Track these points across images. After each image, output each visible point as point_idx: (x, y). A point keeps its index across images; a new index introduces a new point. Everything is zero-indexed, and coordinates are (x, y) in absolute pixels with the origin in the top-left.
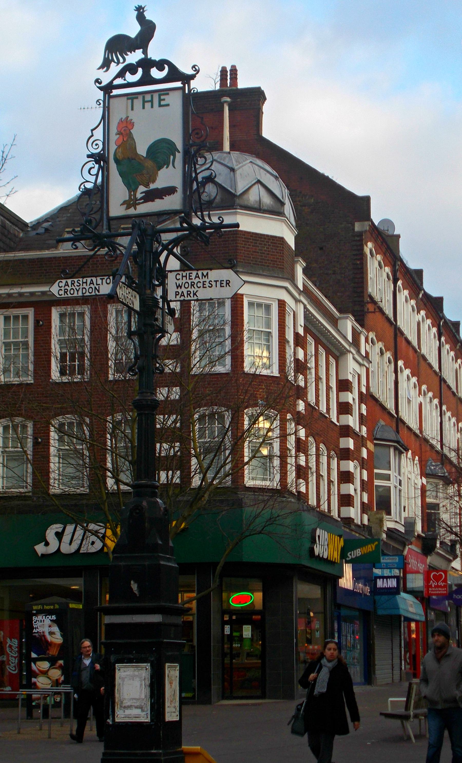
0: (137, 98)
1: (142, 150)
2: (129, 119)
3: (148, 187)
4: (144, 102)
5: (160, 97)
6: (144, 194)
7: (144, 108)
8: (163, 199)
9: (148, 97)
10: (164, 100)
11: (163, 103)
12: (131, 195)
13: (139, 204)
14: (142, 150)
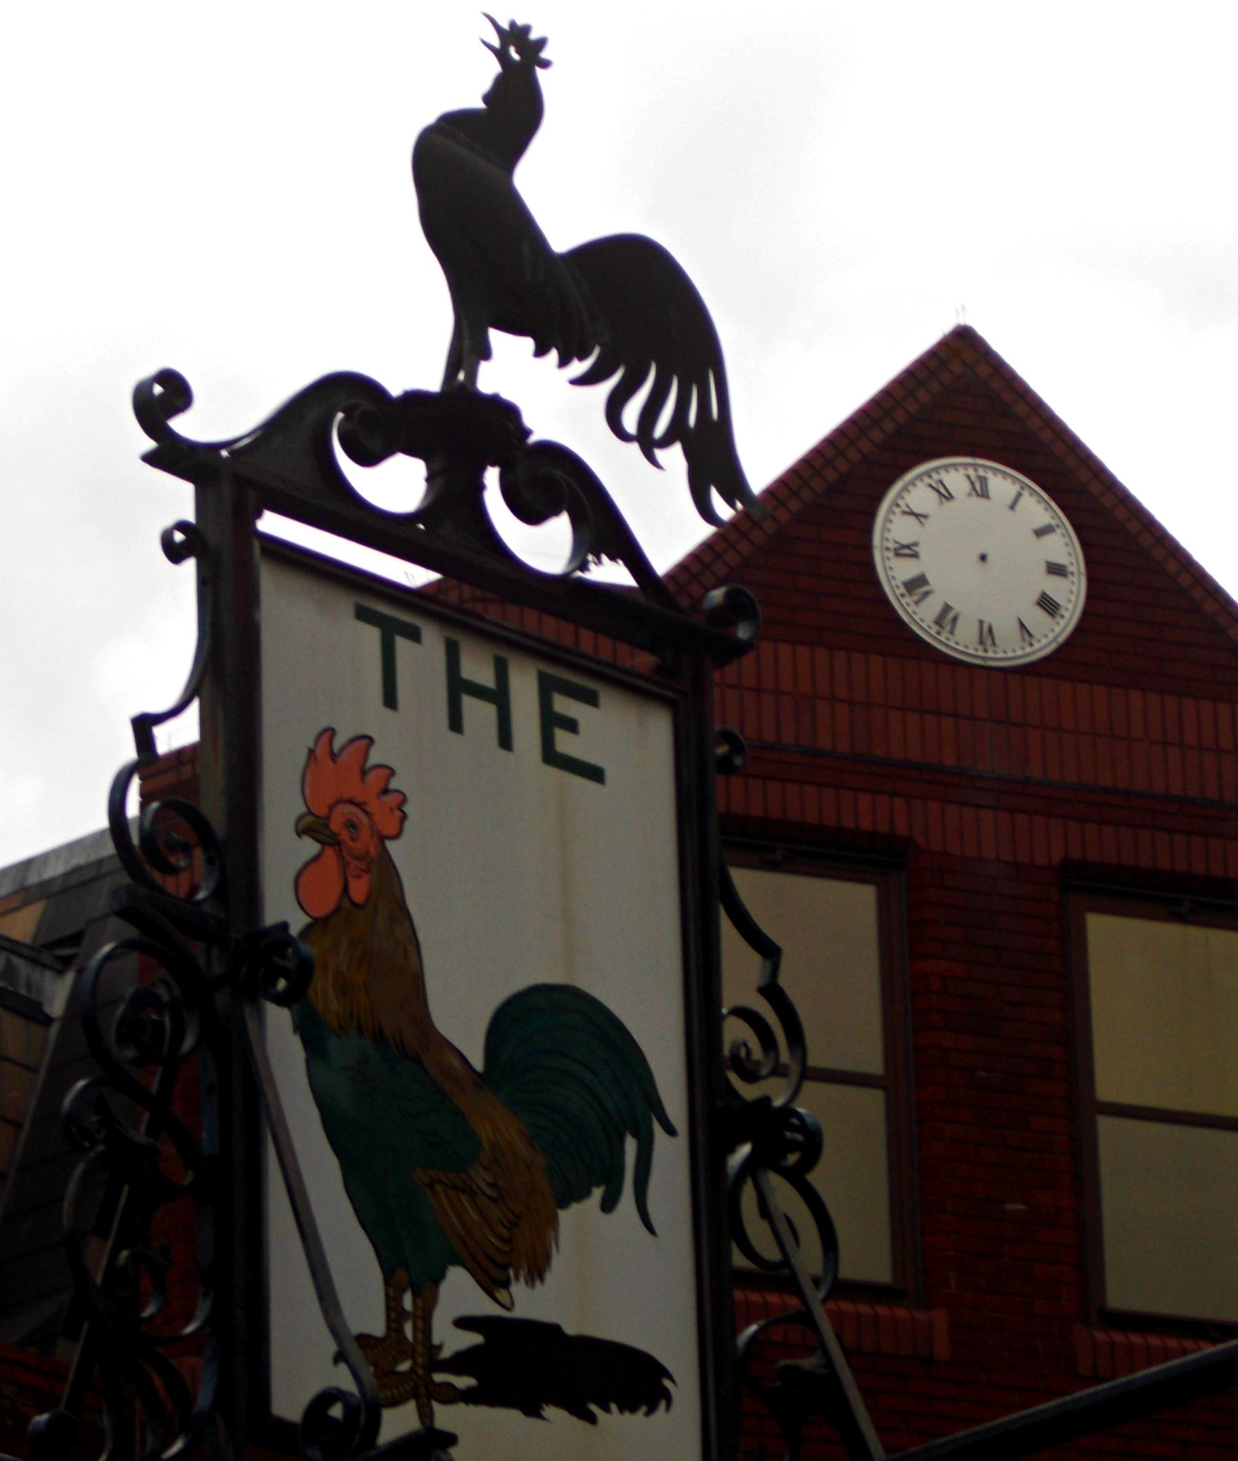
0: (414, 635)
3: (502, 1295)
4: (458, 687)
6: (476, 1339)
7: (456, 724)
8: (592, 1419)
10: (571, 726)
11: (565, 743)
14: (461, 1016)
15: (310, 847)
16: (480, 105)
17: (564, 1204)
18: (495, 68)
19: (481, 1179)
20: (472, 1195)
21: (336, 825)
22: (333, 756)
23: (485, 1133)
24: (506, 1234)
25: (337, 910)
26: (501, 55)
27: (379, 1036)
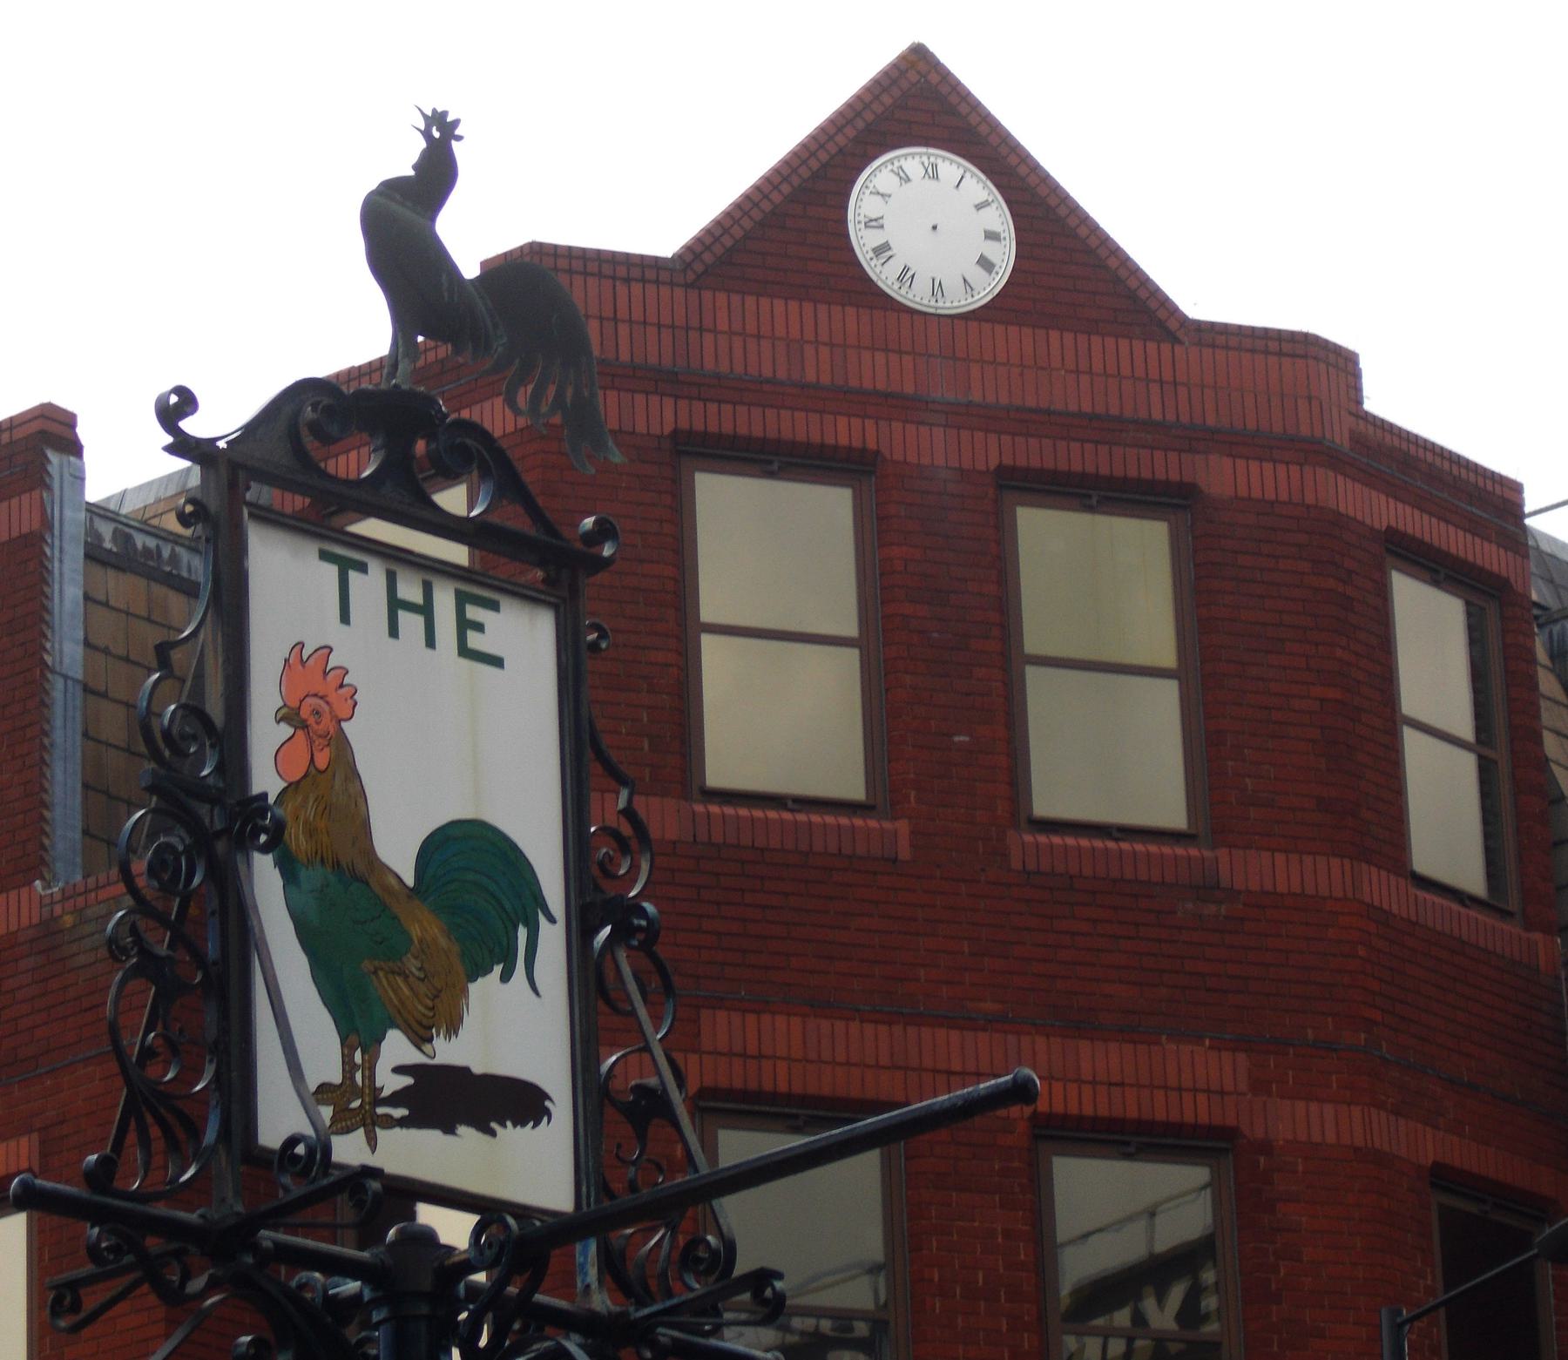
0: (362, 568)
3: (427, 1048)
4: (395, 605)
5: (460, 612)
6: (407, 1081)
7: (394, 632)
8: (493, 1133)
10: (479, 627)
11: (474, 640)
12: (354, 1067)
13: (389, 1123)
14: (397, 848)
15: (286, 731)
16: (411, 173)
17: (473, 978)
18: (422, 144)
19: (412, 965)
20: (406, 977)
21: (305, 713)
22: (303, 663)
23: (415, 932)
24: (430, 1003)
25: (305, 776)
26: (427, 134)
27: (337, 865)
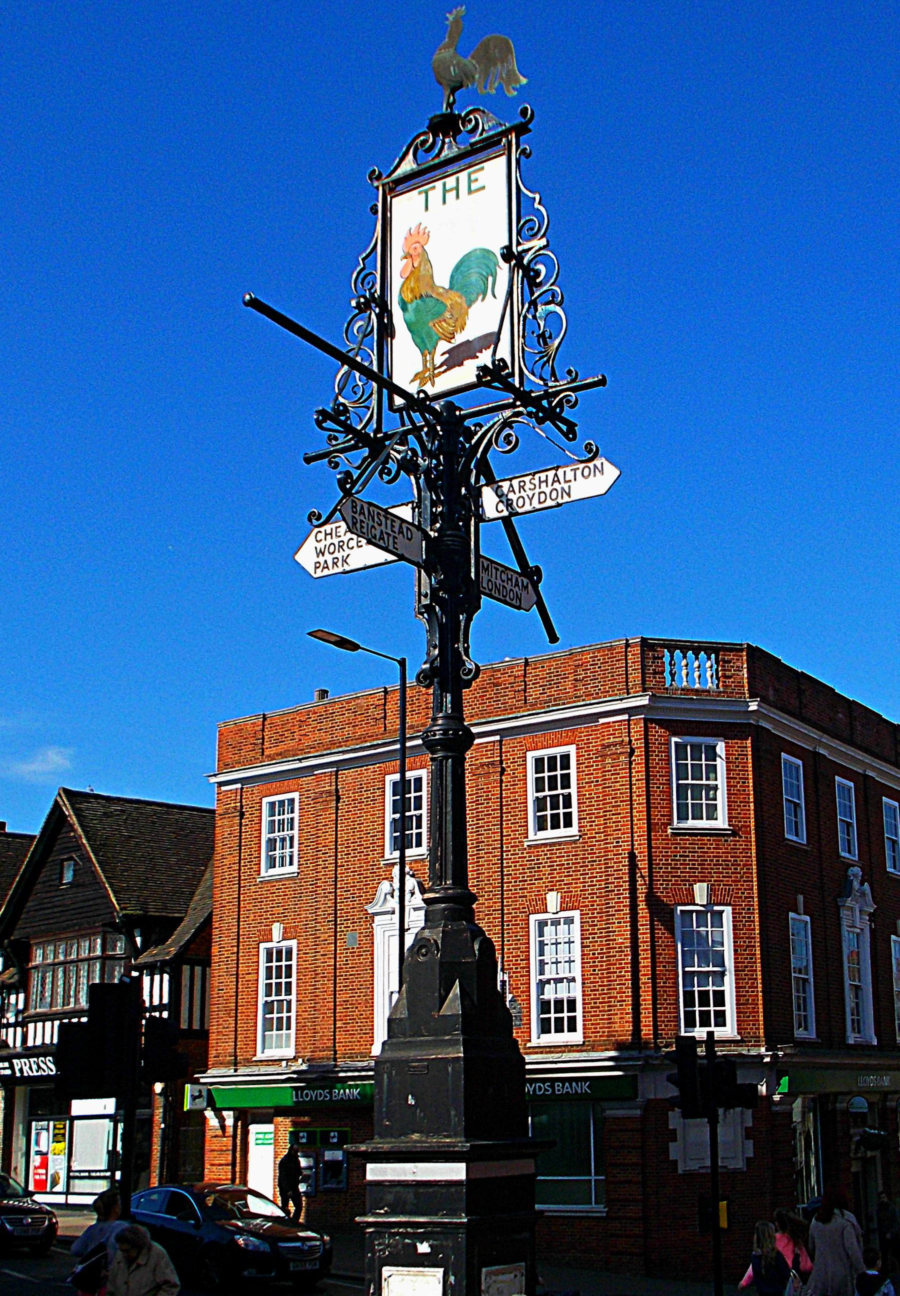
0: (434, 188)
1: (442, 279)
2: (422, 227)
3: (453, 341)
4: (445, 191)
9: (451, 182)
10: (476, 180)
11: (474, 186)
